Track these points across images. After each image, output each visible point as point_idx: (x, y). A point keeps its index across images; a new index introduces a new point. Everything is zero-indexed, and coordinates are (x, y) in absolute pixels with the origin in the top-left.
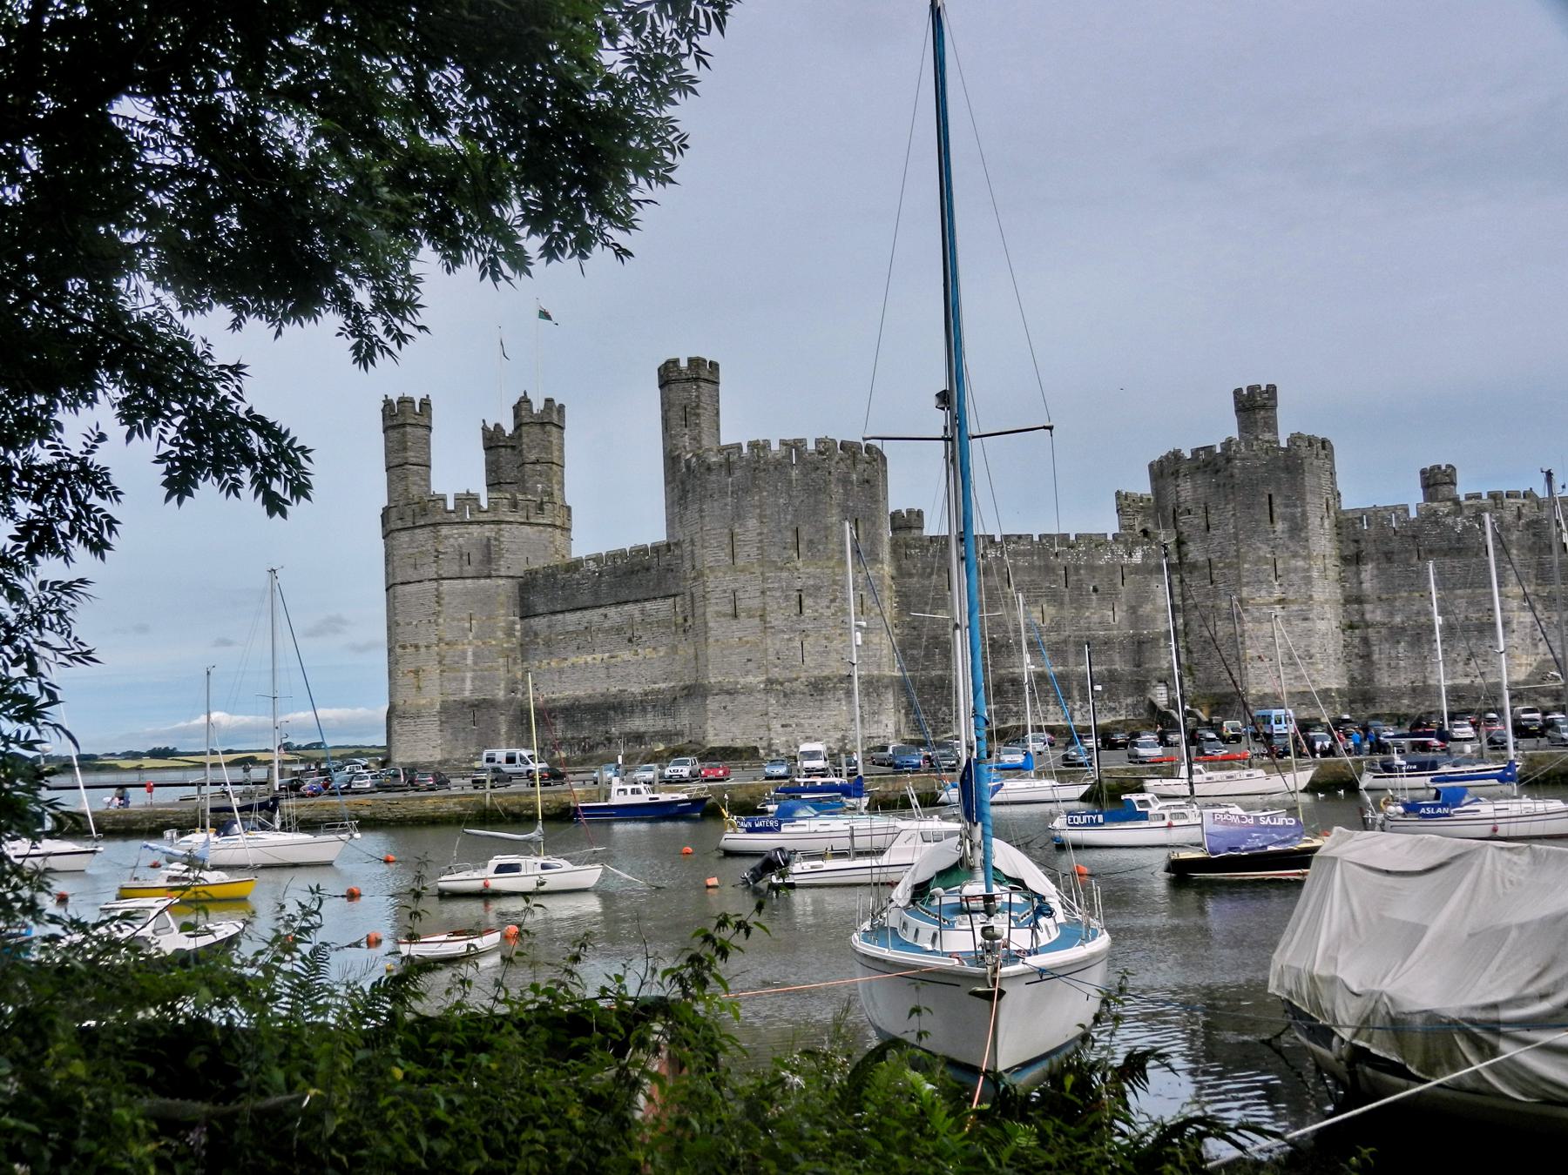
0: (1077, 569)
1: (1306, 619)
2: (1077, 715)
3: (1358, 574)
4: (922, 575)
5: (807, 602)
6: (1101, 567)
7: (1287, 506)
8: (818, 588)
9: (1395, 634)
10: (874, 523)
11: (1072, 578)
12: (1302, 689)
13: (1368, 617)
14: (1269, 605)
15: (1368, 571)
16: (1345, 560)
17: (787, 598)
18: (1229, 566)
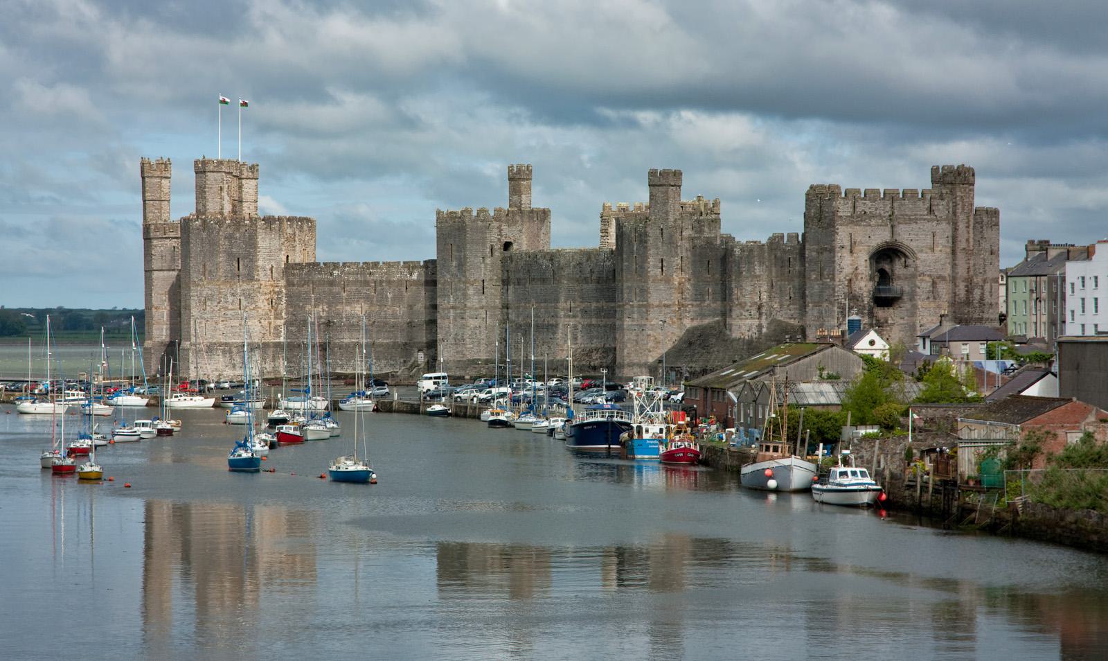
0: (381, 282)
1: (463, 318)
4: (299, 285)
5: (208, 303)
8: (212, 296)
10: (251, 260)
11: (379, 288)
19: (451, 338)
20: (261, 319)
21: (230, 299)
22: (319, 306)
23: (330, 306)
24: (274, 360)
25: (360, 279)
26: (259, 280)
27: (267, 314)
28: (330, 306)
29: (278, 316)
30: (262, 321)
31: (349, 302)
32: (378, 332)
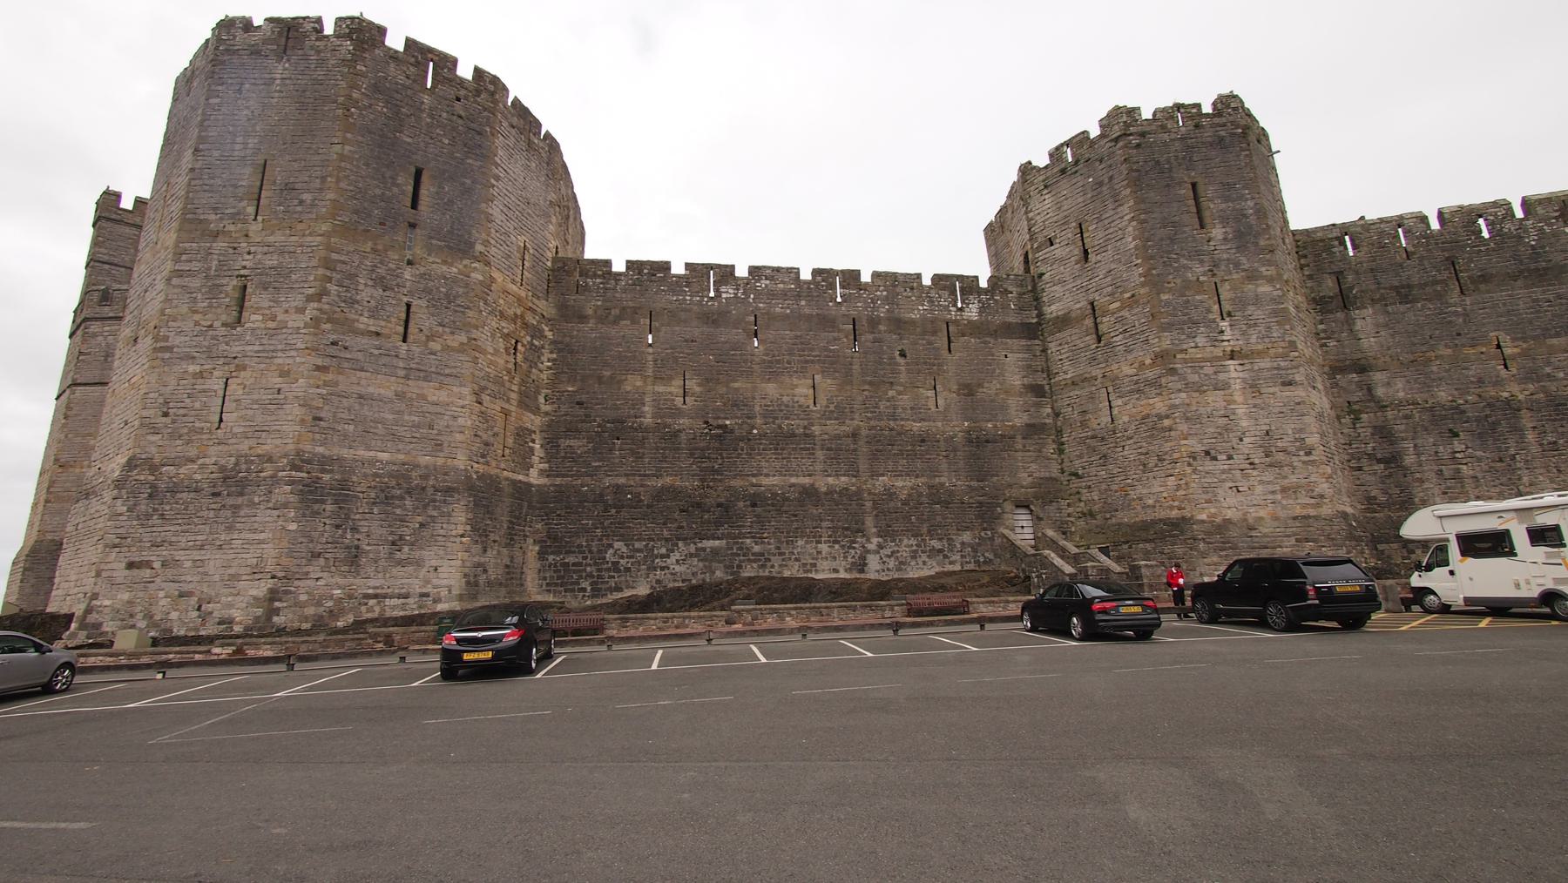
0: (874, 323)
2: (873, 563)
3: (1350, 323)
5: (255, 299)
6: (913, 322)
7: (1226, 199)
8: (282, 272)
9: (1446, 421)
10: (468, 191)
12: (1298, 511)
13: (1380, 392)
14: (1213, 360)
15: (1366, 320)
16: (1320, 304)
17: (214, 291)
18: (1133, 301)
19: (1247, 445)
20: (483, 389)
21: (367, 293)
22: (671, 378)
23: (708, 380)
24: (511, 539)
25: (807, 311)
26: (488, 264)
27: (498, 381)
28: (708, 380)
29: (527, 401)
30: (486, 398)
31: (773, 369)
32: (874, 456)
